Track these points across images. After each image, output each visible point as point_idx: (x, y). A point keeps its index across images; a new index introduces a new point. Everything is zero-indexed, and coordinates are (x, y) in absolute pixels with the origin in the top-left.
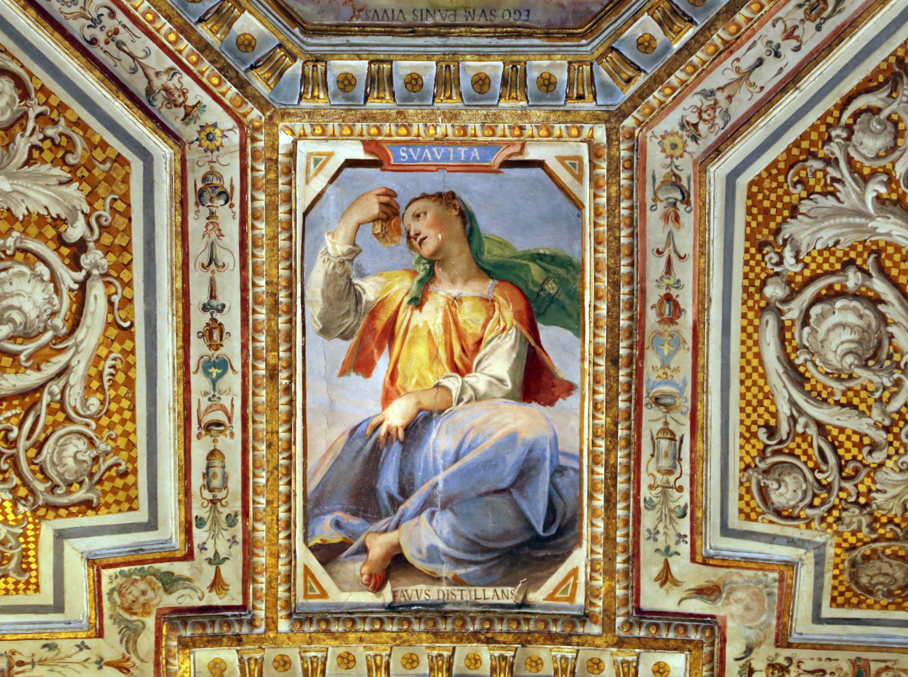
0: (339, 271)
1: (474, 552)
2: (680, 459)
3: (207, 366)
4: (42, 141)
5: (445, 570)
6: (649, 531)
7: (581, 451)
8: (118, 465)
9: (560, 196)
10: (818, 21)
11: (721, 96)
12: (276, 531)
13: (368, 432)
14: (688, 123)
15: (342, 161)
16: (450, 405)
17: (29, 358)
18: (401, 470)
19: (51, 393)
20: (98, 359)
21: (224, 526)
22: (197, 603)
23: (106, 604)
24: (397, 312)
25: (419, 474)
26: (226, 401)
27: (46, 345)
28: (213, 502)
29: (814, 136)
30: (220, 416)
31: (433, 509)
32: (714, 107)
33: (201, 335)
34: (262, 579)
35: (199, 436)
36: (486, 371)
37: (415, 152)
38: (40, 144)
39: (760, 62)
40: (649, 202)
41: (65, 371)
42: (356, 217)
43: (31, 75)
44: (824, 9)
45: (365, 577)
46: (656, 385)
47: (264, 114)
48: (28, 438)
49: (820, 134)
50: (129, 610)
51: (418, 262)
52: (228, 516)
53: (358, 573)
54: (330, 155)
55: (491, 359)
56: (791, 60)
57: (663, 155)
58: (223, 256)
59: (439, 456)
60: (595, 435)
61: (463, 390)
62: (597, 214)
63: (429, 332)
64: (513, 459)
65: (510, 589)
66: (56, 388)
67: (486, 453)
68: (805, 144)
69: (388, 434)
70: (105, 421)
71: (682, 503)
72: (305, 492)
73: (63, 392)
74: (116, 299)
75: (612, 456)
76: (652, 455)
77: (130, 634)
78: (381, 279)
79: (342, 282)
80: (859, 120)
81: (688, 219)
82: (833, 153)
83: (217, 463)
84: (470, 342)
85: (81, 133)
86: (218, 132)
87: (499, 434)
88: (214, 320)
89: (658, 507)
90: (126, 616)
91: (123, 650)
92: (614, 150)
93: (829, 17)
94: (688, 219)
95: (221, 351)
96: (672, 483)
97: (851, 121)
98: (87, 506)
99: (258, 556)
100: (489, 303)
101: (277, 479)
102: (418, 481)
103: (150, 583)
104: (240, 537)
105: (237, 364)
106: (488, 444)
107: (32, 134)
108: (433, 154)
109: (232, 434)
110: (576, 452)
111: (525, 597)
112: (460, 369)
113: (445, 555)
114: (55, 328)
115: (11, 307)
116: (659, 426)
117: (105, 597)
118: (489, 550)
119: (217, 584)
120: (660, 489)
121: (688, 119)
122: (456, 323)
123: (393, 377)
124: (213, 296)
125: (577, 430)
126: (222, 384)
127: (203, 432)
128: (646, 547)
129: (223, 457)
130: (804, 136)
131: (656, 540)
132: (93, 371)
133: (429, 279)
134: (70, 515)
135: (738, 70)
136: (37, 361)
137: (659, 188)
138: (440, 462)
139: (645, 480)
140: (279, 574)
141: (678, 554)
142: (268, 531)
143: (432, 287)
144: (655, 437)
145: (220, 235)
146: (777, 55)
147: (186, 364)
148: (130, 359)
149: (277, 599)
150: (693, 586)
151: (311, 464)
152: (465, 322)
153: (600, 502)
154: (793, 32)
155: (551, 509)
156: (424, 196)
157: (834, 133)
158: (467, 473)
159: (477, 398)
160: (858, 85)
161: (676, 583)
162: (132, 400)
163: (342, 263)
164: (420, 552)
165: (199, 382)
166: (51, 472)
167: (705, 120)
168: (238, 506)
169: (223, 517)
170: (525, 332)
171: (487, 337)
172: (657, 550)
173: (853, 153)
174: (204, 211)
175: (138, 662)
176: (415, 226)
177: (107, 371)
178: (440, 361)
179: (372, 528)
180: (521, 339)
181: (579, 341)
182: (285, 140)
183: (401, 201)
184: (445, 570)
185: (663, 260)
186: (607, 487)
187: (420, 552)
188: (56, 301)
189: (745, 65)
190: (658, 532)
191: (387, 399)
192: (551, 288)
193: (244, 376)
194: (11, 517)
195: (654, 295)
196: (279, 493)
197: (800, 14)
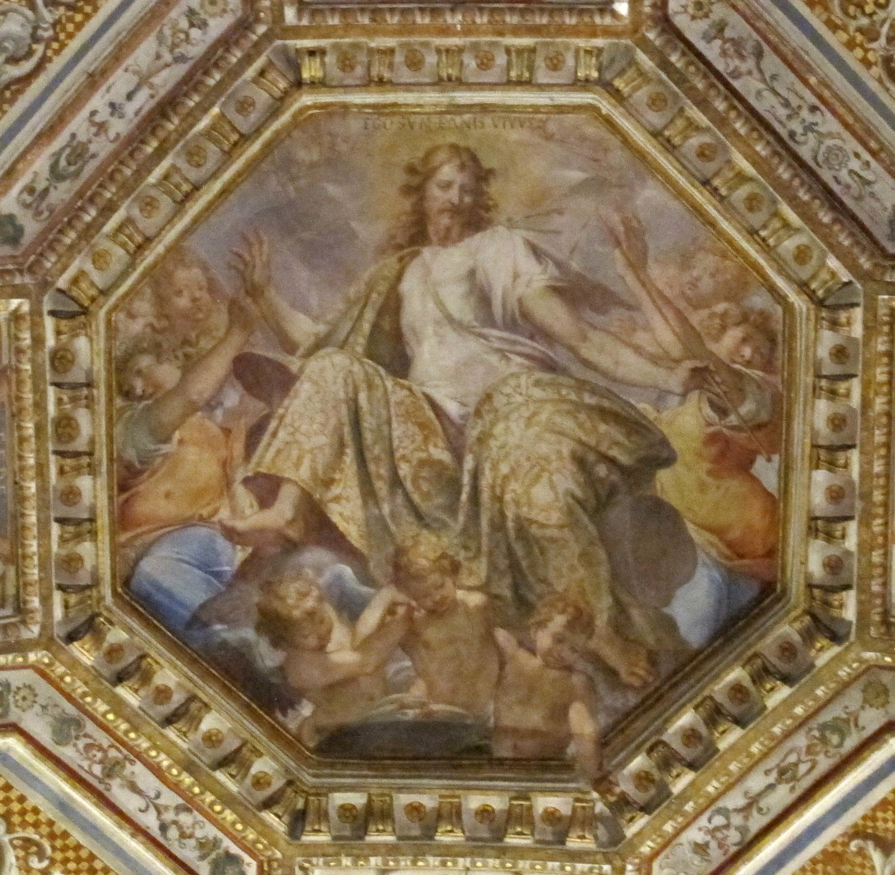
4: (874, 13)
10: (75, 143)
11: (167, 57)
14: (200, 28)
29: (70, 27)
32: (174, 46)
38: (878, 11)
39: (130, 96)
43: (880, 81)
44: (69, 155)
47: (644, 36)
49: (63, 29)
56: (98, 102)
68: (79, 18)
80: (26, 49)
82: (50, 11)
85: (833, 18)
86: (691, 10)
93: (63, 149)
97: (35, 46)
107: (884, 21)
121: (199, 32)
130: (79, 26)
135: (151, 86)
146: (112, 105)
154: (99, 130)
157: (50, 33)
160: (30, 84)
173: (29, 14)
189: (144, 94)
197: (93, 148)
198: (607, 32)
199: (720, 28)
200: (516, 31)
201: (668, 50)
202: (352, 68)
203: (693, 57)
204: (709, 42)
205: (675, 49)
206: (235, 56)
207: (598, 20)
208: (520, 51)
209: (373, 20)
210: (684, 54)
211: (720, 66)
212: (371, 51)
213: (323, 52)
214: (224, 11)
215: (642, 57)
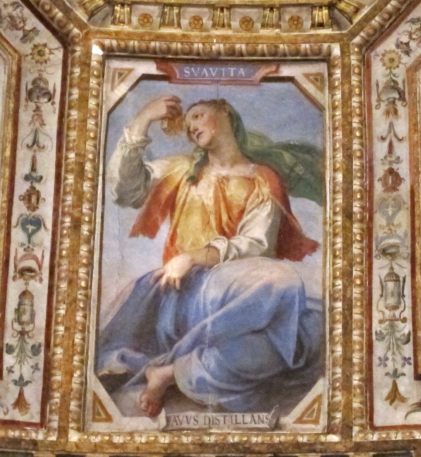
0: (133, 155)
1: (235, 383)
2: (404, 296)
3: (25, 223)
5: (211, 399)
6: (380, 359)
7: (324, 297)
9: (307, 102)
12: (71, 353)
13: (152, 282)
14: (402, 43)
15: (139, 75)
16: (218, 261)
18: (177, 315)
21: (30, 354)
24: (177, 188)
25: (191, 317)
26: (38, 253)
28: (22, 333)
30: (32, 264)
31: (203, 346)
34: (57, 395)
35: (14, 278)
36: (248, 234)
37: (196, 70)
40: (374, 103)
42: (149, 115)
45: (143, 406)
46: (383, 239)
47: (81, 31)
51: (195, 150)
52: (33, 347)
53: (138, 401)
54: (130, 71)
55: (251, 225)
57: (384, 68)
58: (42, 139)
59: (208, 302)
60: (335, 278)
62: (334, 108)
63: (203, 204)
64: (269, 305)
65: (265, 414)
67: (245, 301)
69: (167, 283)
71: (406, 331)
72: (97, 331)
75: (349, 292)
76: (381, 296)
78: (166, 162)
79: (136, 163)
81: (402, 110)
83: (27, 302)
84: (235, 212)
86: (47, 51)
87: (258, 285)
88: (33, 188)
89: (387, 337)
92: (346, 60)
94: (402, 110)
95: (37, 212)
96: (397, 315)
99: (55, 375)
100: (250, 182)
101: (75, 311)
102: (190, 323)
104: (41, 366)
105: (49, 224)
108: (209, 72)
109: (41, 280)
110: (319, 296)
111: (278, 420)
113: (212, 385)
116: (386, 271)
118: (249, 381)
120: (387, 323)
121: (401, 40)
122: (225, 198)
123: (173, 238)
125: (320, 280)
126: (36, 238)
127: (18, 276)
128: (378, 373)
129: (32, 297)
131: (386, 365)
137: (382, 92)
139: (376, 316)
140: (72, 390)
141: (404, 374)
142: (64, 354)
143: (206, 169)
144: (383, 281)
145: (43, 124)
149: (69, 411)
150: (416, 401)
151: (103, 308)
152: (231, 196)
153: (339, 329)
156: (202, 102)
161: (403, 400)
163: (136, 149)
164: (190, 383)
167: (414, 39)
168: (41, 339)
169: (29, 347)
170: (279, 204)
171: (249, 207)
172: (387, 374)
174: (32, 105)
176: (193, 124)
178: (211, 227)
179: (151, 362)
180: (276, 211)
181: (321, 209)
182: (97, 51)
183: (184, 106)
184: (211, 399)
185: (386, 144)
186: (345, 317)
187: (190, 383)
190: (387, 359)
191: (168, 256)
192: (300, 170)
193: (54, 234)
195: (380, 171)
196: (76, 322)
198: (109, 34)
199: (25, 38)
200: (173, 38)
201: (65, 20)
202: (292, 18)
203: (46, 16)
204: (34, 28)
205: (59, 21)
206: (376, 21)
207: (114, 43)
208: (171, 24)
209: (277, 47)
210: (53, 18)
211: (27, 12)
212: (278, 26)
213: (313, 26)
214: (383, 55)
215: (83, 17)
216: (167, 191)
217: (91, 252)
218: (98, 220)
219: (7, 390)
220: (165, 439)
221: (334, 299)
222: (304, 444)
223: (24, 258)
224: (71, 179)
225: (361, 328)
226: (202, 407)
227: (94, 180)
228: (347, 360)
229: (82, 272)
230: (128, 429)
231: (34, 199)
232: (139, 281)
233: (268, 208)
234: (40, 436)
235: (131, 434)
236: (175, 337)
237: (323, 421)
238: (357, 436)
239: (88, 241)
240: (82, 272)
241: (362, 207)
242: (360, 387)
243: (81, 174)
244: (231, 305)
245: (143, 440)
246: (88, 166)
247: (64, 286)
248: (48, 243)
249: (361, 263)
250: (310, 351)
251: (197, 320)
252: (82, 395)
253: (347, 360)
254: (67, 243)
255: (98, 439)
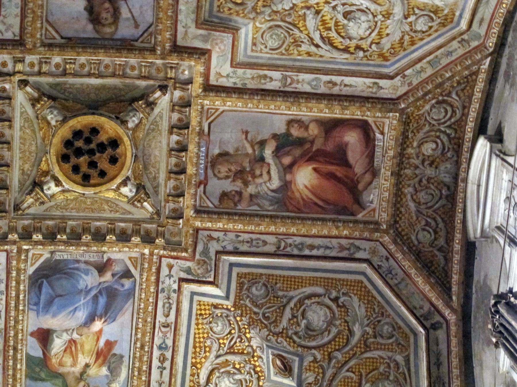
0: (115, 378)
3: (166, 348)
5: (82, 266)
7: (28, 311)
8: (203, 319)
16: (77, 329)
17: (230, 365)
19: (223, 350)
20: (206, 358)
21: (166, 289)
22: (179, 261)
23: (213, 266)
24: (95, 362)
25: (90, 303)
26: (161, 334)
27: (223, 367)
28: (169, 298)
30: (163, 329)
33: (167, 359)
35: (172, 323)
41: (218, 357)
45: (114, 264)
48: (233, 337)
50: (205, 262)
51: (86, 379)
55: (61, 345)
60: (22, 320)
61: (72, 333)
63: (83, 354)
64: (54, 308)
66: (221, 352)
69: (101, 319)
70: (206, 335)
73: (219, 350)
74: (196, 377)
77: (205, 252)
79: (114, 374)
83: (166, 312)
84: (68, 351)
88: (162, 364)
90: (206, 260)
91: (209, 245)
95: (161, 352)
98: (216, 307)
100: (61, 364)
101: (144, 308)
102: (91, 301)
103: (196, 272)
104: (160, 284)
105: (155, 347)
106: (64, 313)
109: (159, 322)
110: (30, 312)
112: (72, 342)
113: (82, 272)
114: (219, 372)
115: (233, 384)
117: (213, 269)
118: (65, 273)
119: (170, 267)
122: (73, 357)
123: (98, 340)
124: (162, 372)
125: (30, 320)
126: (161, 341)
132: (208, 354)
133: (82, 374)
134: (222, 305)
136: (226, 363)
138: (82, 307)
142: (149, 289)
143: (82, 370)
147: (173, 350)
148: (194, 356)
149: (148, 263)
151: (131, 309)
153: (21, 297)
155: (40, 288)
158: (73, 304)
159: (66, 331)
162: (195, 341)
163: (114, 380)
164: (92, 273)
165: (169, 343)
166: (227, 322)
168: (160, 295)
170: (48, 354)
171: (62, 353)
175: (204, 239)
177: (202, 353)
179: (109, 284)
180: (49, 351)
184: (82, 266)
187: (92, 273)
188: (217, 382)
191: (100, 332)
192: (37, 369)
193: (153, 343)
194: (244, 309)
216: (100, 361)
217: (136, 334)
218: (132, 348)
219: (177, 273)
220: (105, 249)
221: (23, 311)
222: (40, 245)
223: (167, 332)
224: (144, 368)
225: (11, 297)
226: (86, 262)
227: (133, 367)
228: (18, 283)
229: (140, 326)
230: (121, 253)
231: (162, 358)
232: (114, 320)
233: (53, 352)
234: (162, 252)
235: (120, 251)
236: (98, 295)
237: (30, 255)
238: (15, 248)
239: (137, 340)
240: (140, 326)
241: (8, 352)
242: (12, 270)
243: (140, 370)
244: (72, 308)
245: (114, 249)
246: (136, 373)
247: (149, 320)
248: (156, 339)
249: (10, 327)
250: (35, 287)
251: (87, 303)
252: (142, 269)
253: (18, 283)
254: (147, 339)
255: (135, 250)
